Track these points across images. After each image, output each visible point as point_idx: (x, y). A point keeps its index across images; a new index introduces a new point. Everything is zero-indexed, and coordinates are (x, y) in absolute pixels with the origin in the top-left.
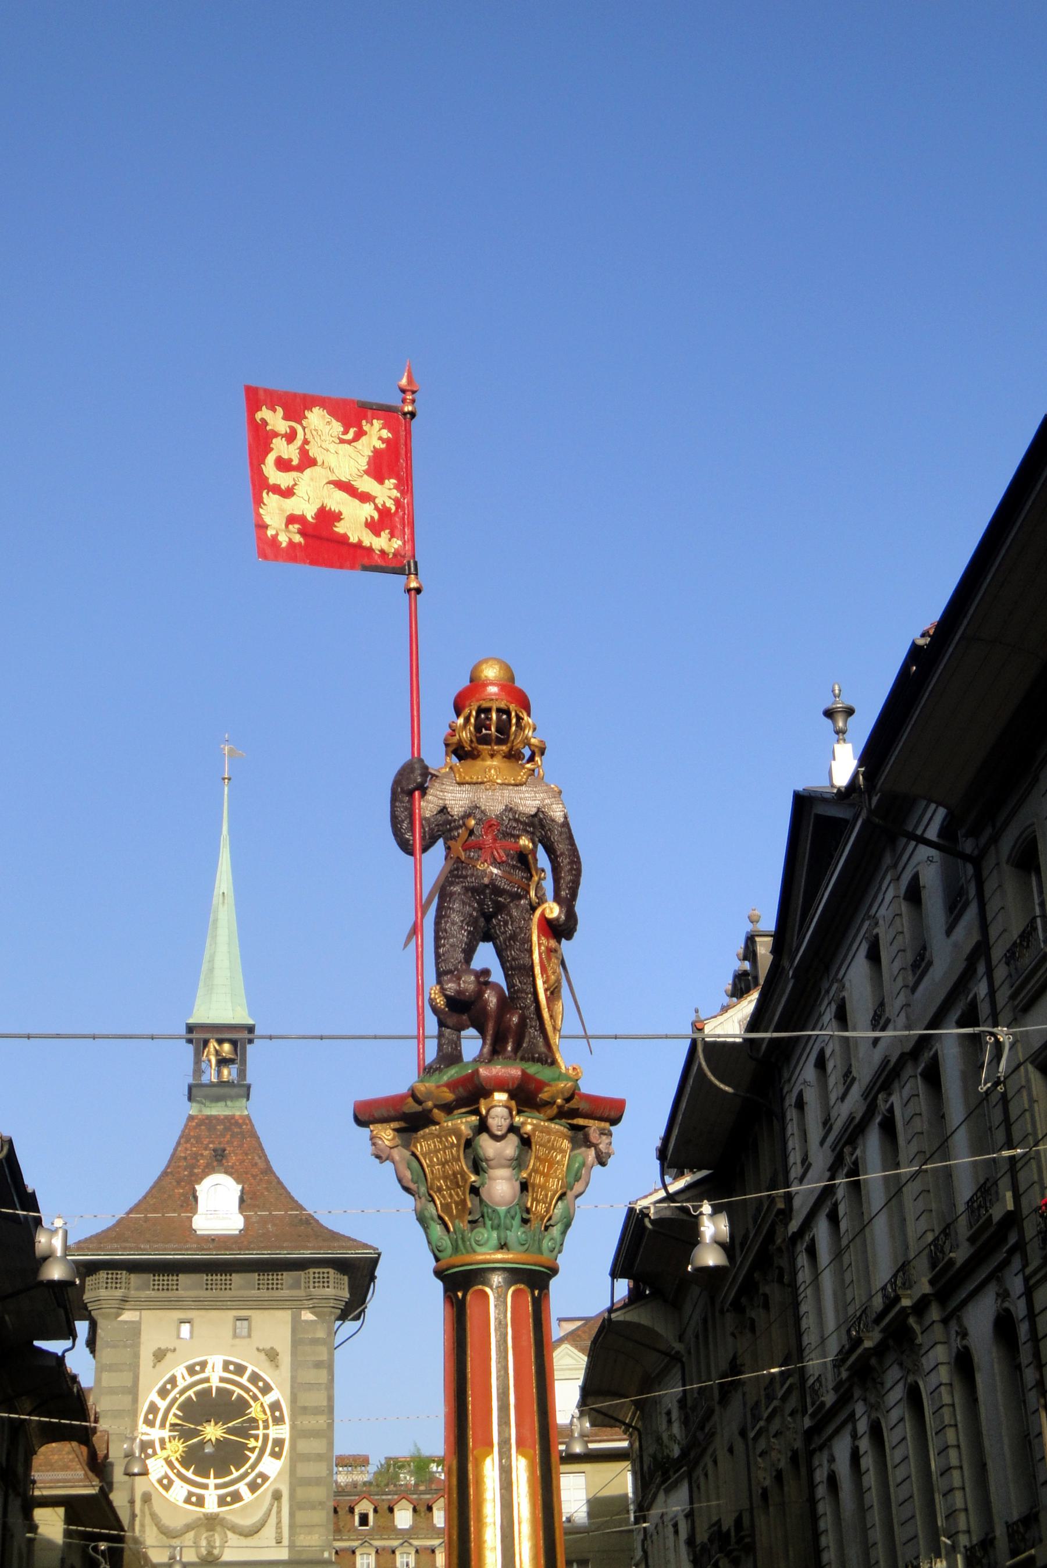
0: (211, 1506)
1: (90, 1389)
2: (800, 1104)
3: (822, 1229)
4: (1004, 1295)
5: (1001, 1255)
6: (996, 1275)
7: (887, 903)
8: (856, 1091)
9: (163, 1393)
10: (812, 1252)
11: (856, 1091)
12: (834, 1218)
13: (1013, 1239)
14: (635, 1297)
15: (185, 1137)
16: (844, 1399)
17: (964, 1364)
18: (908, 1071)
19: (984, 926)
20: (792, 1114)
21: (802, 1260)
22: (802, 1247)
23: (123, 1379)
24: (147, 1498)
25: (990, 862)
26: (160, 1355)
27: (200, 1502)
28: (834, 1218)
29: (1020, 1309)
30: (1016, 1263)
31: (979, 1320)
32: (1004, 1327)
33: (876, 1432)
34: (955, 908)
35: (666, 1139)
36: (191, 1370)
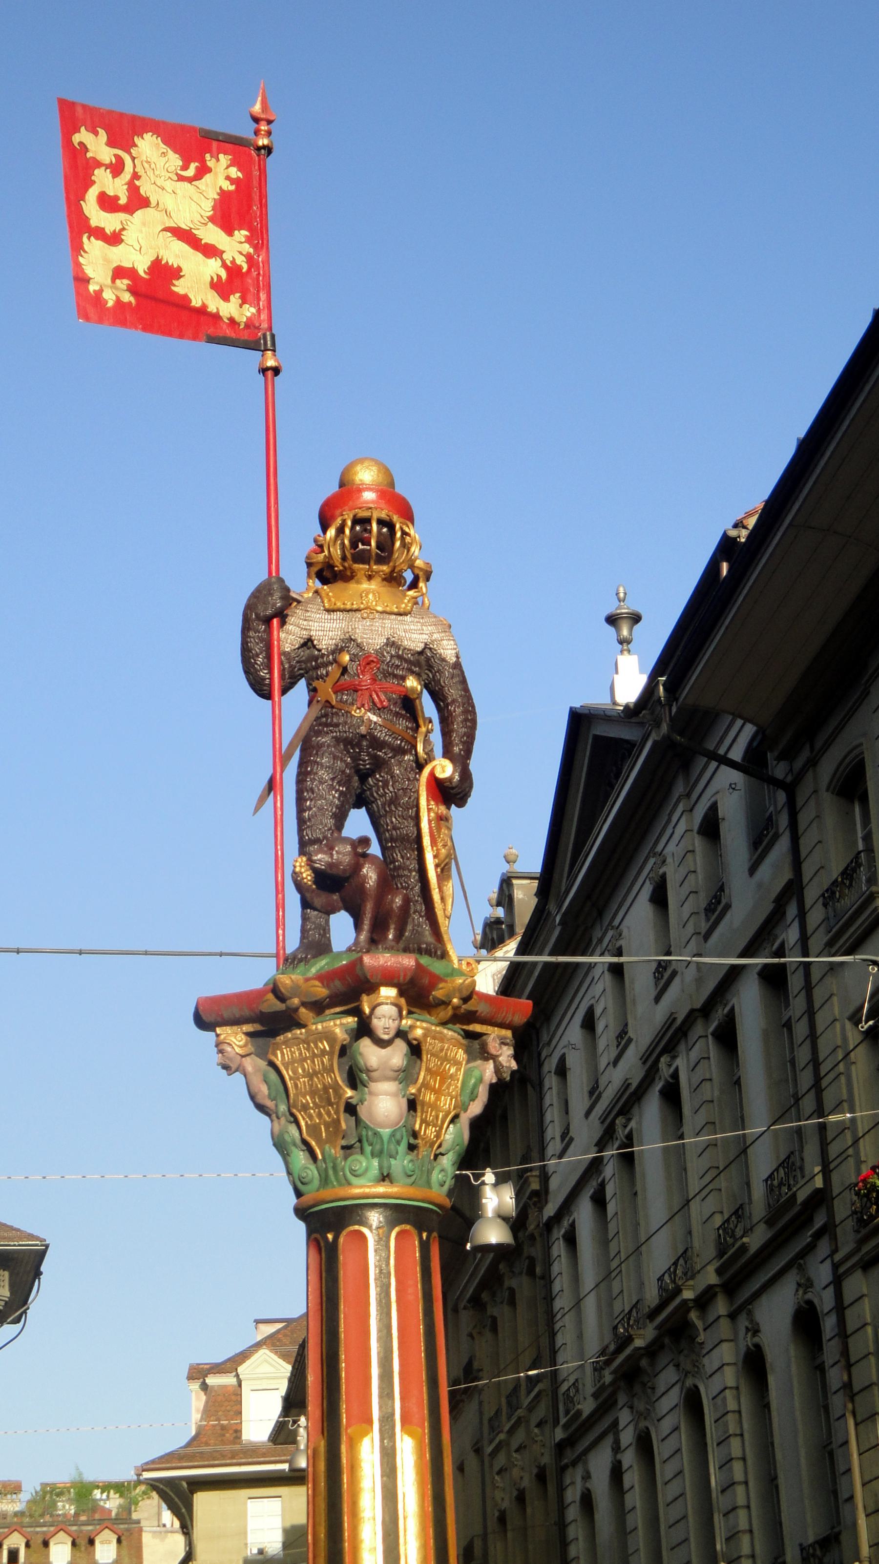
3: (584, 1214)
4: (807, 1285)
6: (798, 1262)
8: (632, 1055)
10: (571, 1240)
11: (632, 1055)
12: (600, 1201)
17: (755, 1365)
18: (698, 1029)
21: (559, 1248)
22: (558, 1233)
28: (600, 1201)
29: (826, 1300)
30: (824, 1248)
31: (776, 1313)
32: (806, 1322)
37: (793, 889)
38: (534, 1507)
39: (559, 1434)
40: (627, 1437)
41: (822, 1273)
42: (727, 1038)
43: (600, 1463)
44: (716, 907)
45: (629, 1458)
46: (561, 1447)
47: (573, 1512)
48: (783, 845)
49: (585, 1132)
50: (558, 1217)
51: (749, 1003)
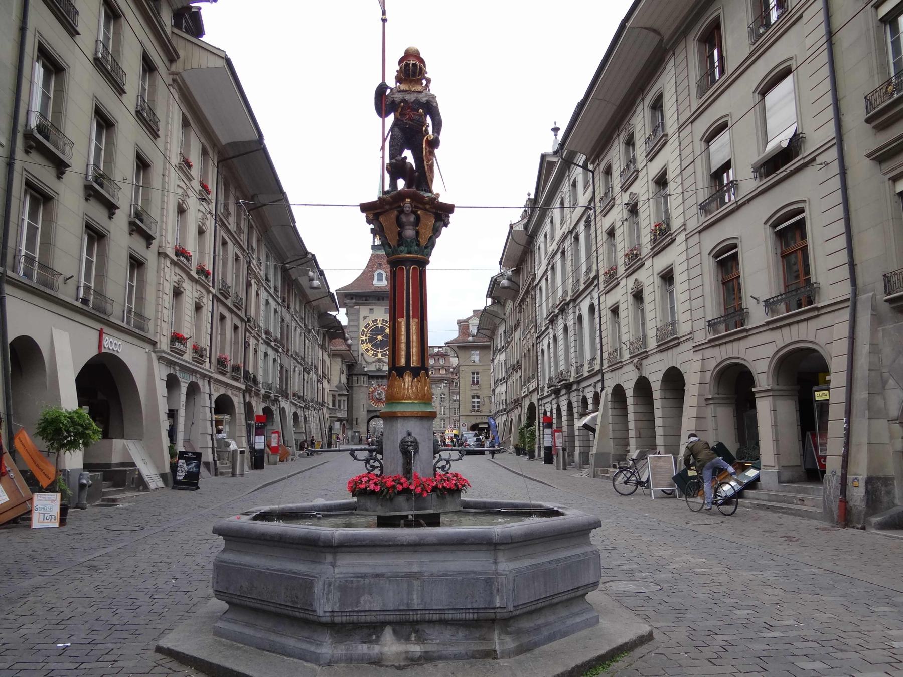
0: (379, 356)
1: (345, 327)
2: (539, 248)
4: (592, 298)
5: (592, 287)
7: (566, 187)
8: (555, 243)
9: (366, 327)
10: (540, 289)
11: (555, 243)
12: (547, 280)
13: (596, 282)
14: (493, 303)
15: (371, 260)
16: (547, 329)
17: (580, 319)
18: (569, 237)
19: (594, 192)
20: (536, 251)
21: (537, 292)
22: (538, 288)
23: (355, 324)
24: (362, 354)
25: (596, 173)
26: (365, 318)
27: (377, 355)
28: (547, 280)
29: (596, 302)
32: (592, 308)
33: (555, 337)
34: (586, 187)
35: (502, 259)
36: (373, 322)
37: (593, 199)
38: (531, 351)
39: (537, 335)
40: (551, 336)
41: (595, 295)
42: (577, 238)
43: (545, 342)
44: (575, 204)
45: (551, 341)
46: (537, 338)
47: (539, 353)
48: (591, 187)
49: (544, 262)
50: (537, 285)
51: (582, 227)
